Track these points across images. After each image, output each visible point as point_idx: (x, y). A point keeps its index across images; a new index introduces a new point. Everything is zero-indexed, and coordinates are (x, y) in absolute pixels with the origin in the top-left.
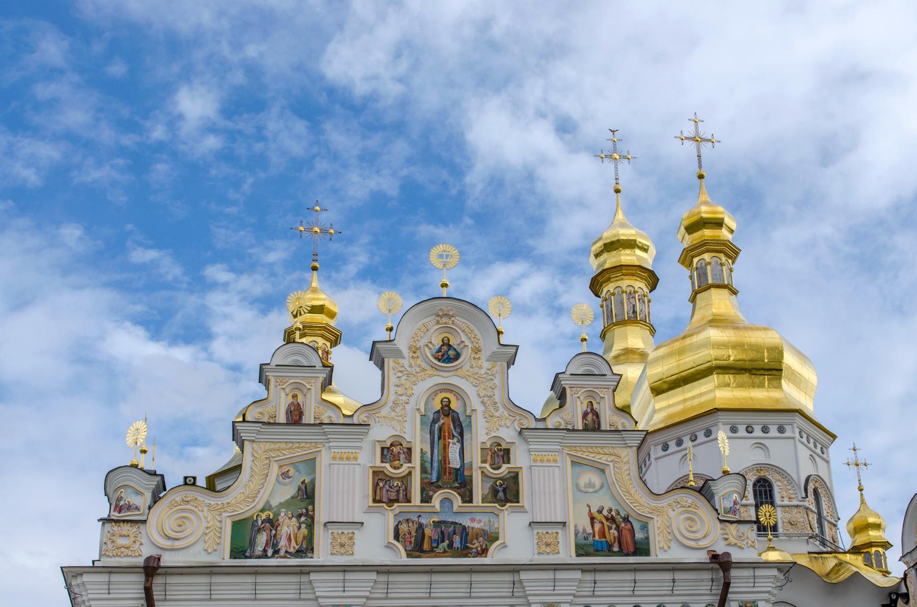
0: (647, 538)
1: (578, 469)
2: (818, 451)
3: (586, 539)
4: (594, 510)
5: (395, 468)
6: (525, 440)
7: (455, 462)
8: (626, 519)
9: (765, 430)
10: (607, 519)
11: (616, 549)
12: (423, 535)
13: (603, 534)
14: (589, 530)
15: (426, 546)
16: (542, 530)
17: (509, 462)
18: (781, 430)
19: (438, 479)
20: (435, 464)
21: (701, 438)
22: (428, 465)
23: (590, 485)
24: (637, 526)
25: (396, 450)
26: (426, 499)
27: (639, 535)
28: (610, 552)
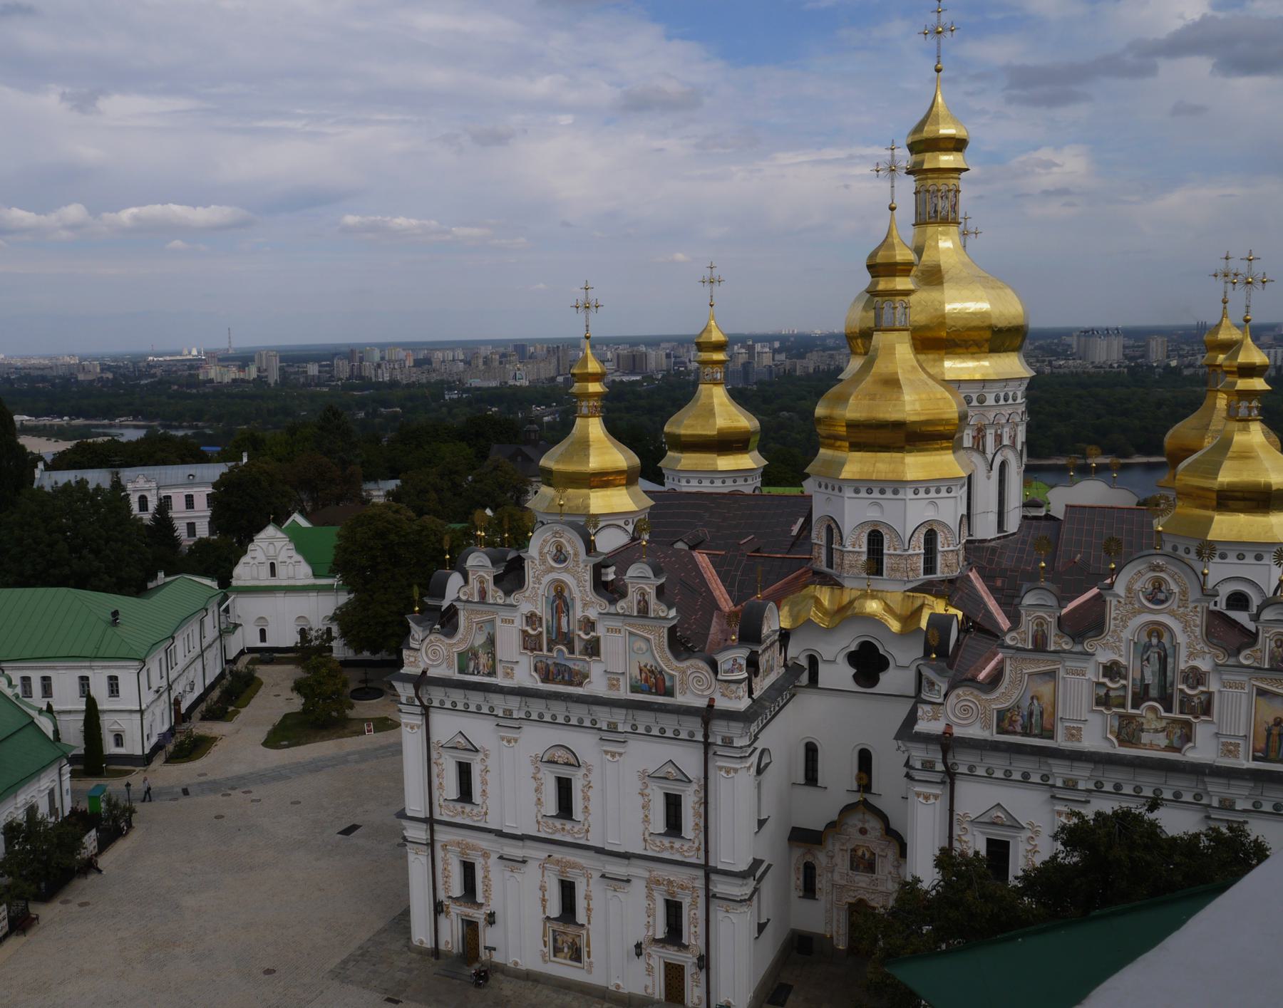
0: (673, 686)
1: (633, 638)
3: (636, 682)
5: (534, 630)
7: (565, 629)
8: (661, 672)
9: (882, 492)
11: (654, 691)
12: (549, 670)
13: (646, 681)
14: (639, 677)
15: (551, 678)
17: (594, 631)
18: (896, 492)
19: (556, 638)
20: (554, 629)
22: (550, 629)
23: (640, 649)
24: (667, 678)
26: (550, 650)
27: (668, 684)
28: (650, 693)
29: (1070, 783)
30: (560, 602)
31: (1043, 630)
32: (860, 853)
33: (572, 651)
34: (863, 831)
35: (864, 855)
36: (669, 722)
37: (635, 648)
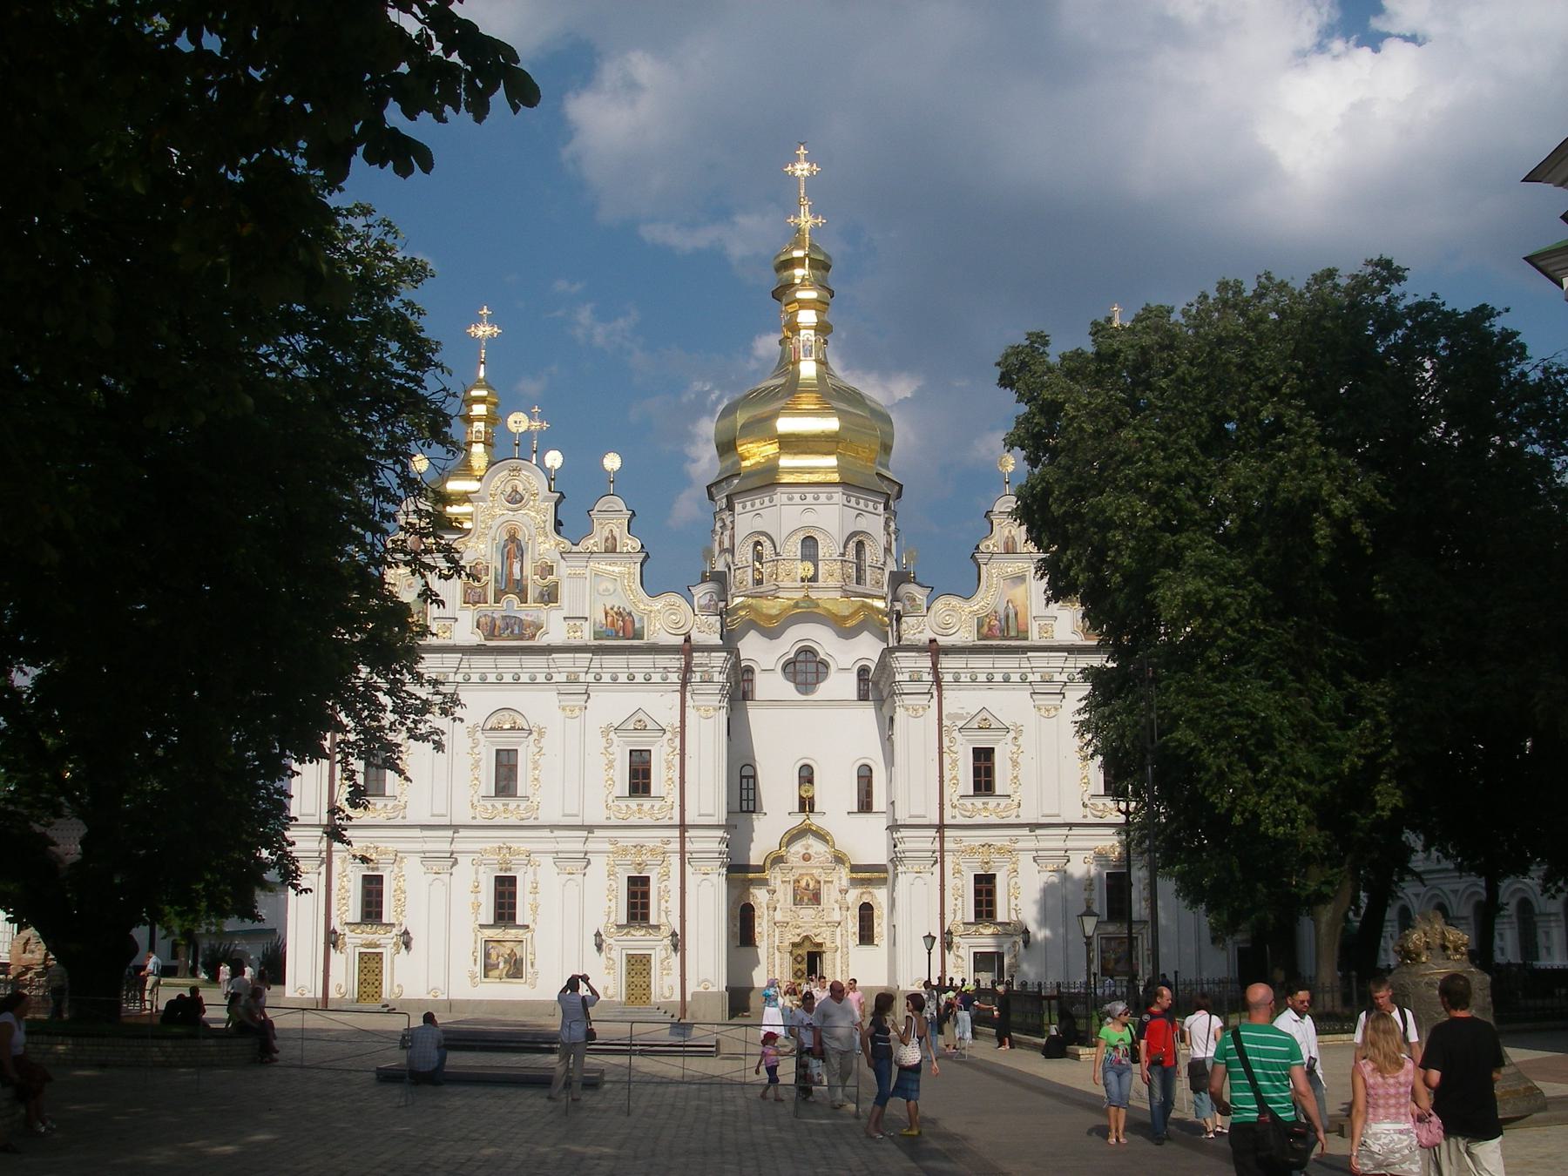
1: (598, 579)
2: (870, 508)
4: (608, 608)
6: (562, 558)
7: (517, 576)
8: (630, 614)
9: (817, 499)
10: (616, 614)
11: (621, 635)
14: (604, 622)
15: (496, 634)
16: (572, 623)
21: (767, 503)
22: (499, 578)
25: (479, 567)
27: (637, 625)
28: (617, 637)
29: (1047, 678)
30: (513, 547)
31: (1013, 537)
32: (803, 883)
33: (524, 600)
34: (807, 858)
35: (808, 885)
36: (641, 662)
37: (601, 590)
